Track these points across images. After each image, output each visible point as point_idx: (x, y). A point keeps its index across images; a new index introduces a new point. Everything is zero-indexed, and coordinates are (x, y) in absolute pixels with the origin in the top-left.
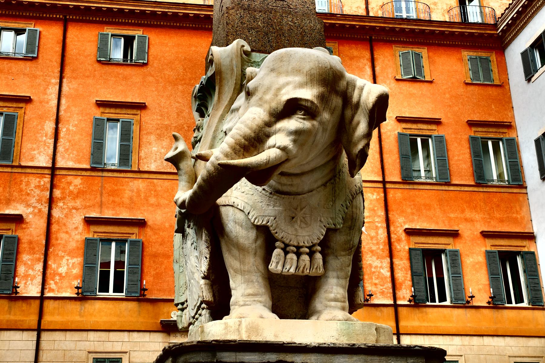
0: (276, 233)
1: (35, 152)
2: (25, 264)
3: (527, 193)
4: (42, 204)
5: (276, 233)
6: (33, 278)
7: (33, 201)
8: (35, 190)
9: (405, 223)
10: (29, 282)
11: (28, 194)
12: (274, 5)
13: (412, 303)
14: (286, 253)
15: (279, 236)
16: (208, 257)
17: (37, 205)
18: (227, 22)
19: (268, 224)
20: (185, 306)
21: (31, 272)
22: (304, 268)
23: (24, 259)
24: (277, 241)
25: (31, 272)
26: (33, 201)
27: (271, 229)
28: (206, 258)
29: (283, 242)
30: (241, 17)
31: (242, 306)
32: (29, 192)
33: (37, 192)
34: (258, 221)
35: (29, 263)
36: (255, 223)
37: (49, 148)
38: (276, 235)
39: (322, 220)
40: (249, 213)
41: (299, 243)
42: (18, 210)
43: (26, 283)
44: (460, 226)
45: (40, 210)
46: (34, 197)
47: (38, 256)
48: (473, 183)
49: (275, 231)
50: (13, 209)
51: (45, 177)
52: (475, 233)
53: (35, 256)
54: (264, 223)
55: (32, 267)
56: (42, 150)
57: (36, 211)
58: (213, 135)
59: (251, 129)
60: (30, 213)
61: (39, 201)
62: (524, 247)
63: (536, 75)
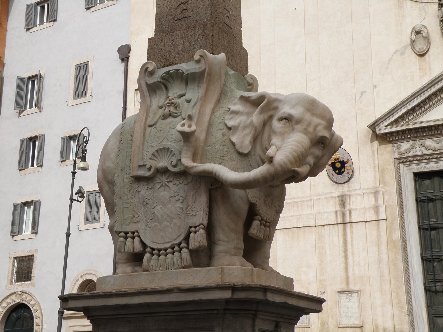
0: (259, 210)
5: (259, 210)
12: (228, 30)
14: (261, 224)
15: (261, 212)
16: (208, 214)
18: (213, 35)
19: (257, 203)
20: (128, 235)
22: (266, 236)
24: (257, 215)
27: (258, 207)
28: (207, 214)
29: (261, 217)
30: (218, 33)
31: (233, 255)
34: (252, 200)
36: (251, 201)
38: (259, 211)
39: (277, 206)
40: (248, 193)
41: (266, 219)
49: (259, 209)
54: (255, 202)
58: (209, 122)
59: (305, 149)
63: (35, 29)
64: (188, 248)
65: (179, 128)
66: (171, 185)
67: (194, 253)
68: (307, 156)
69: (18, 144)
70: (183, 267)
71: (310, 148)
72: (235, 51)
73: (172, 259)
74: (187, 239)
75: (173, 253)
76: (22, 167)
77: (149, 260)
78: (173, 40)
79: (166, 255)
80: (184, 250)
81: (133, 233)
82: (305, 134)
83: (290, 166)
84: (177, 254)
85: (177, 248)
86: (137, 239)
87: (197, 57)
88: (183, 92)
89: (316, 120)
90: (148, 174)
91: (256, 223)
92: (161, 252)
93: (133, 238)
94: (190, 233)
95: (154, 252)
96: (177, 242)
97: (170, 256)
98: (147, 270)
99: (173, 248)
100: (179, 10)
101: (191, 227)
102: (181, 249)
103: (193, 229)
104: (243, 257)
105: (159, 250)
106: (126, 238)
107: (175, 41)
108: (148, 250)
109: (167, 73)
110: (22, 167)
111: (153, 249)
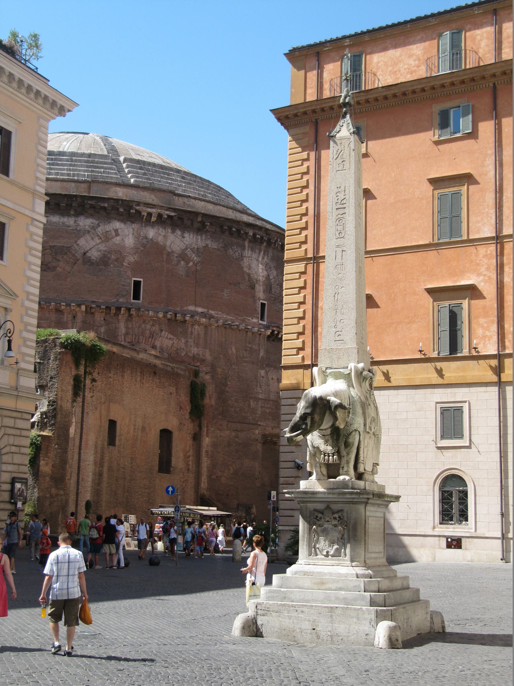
1: (480, 224)
2: (482, 327)
4: (491, 272)
6: (490, 338)
7: (483, 269)
8: (484, 260)
10: (487, 342)
11: (478, 264)
17: (486, 273)
21: (488, 333)
23: (481, 322)
25: (488, 333)
26: (483, 269)
32: (478, 262)
33: (485, 261)
35: (485, 325)
37: (491, 218)
42: (471, 279)
43: (484, 344)
45: (489, 277)
46: (483, 266)
47: (492, 318)
50: (467, 280)
51: (491, 246)
53: (489, 319)
55: (488, 329)
56: (486, 221)
57: (486, 278)
60: (481, 281)
61: (488, 269)
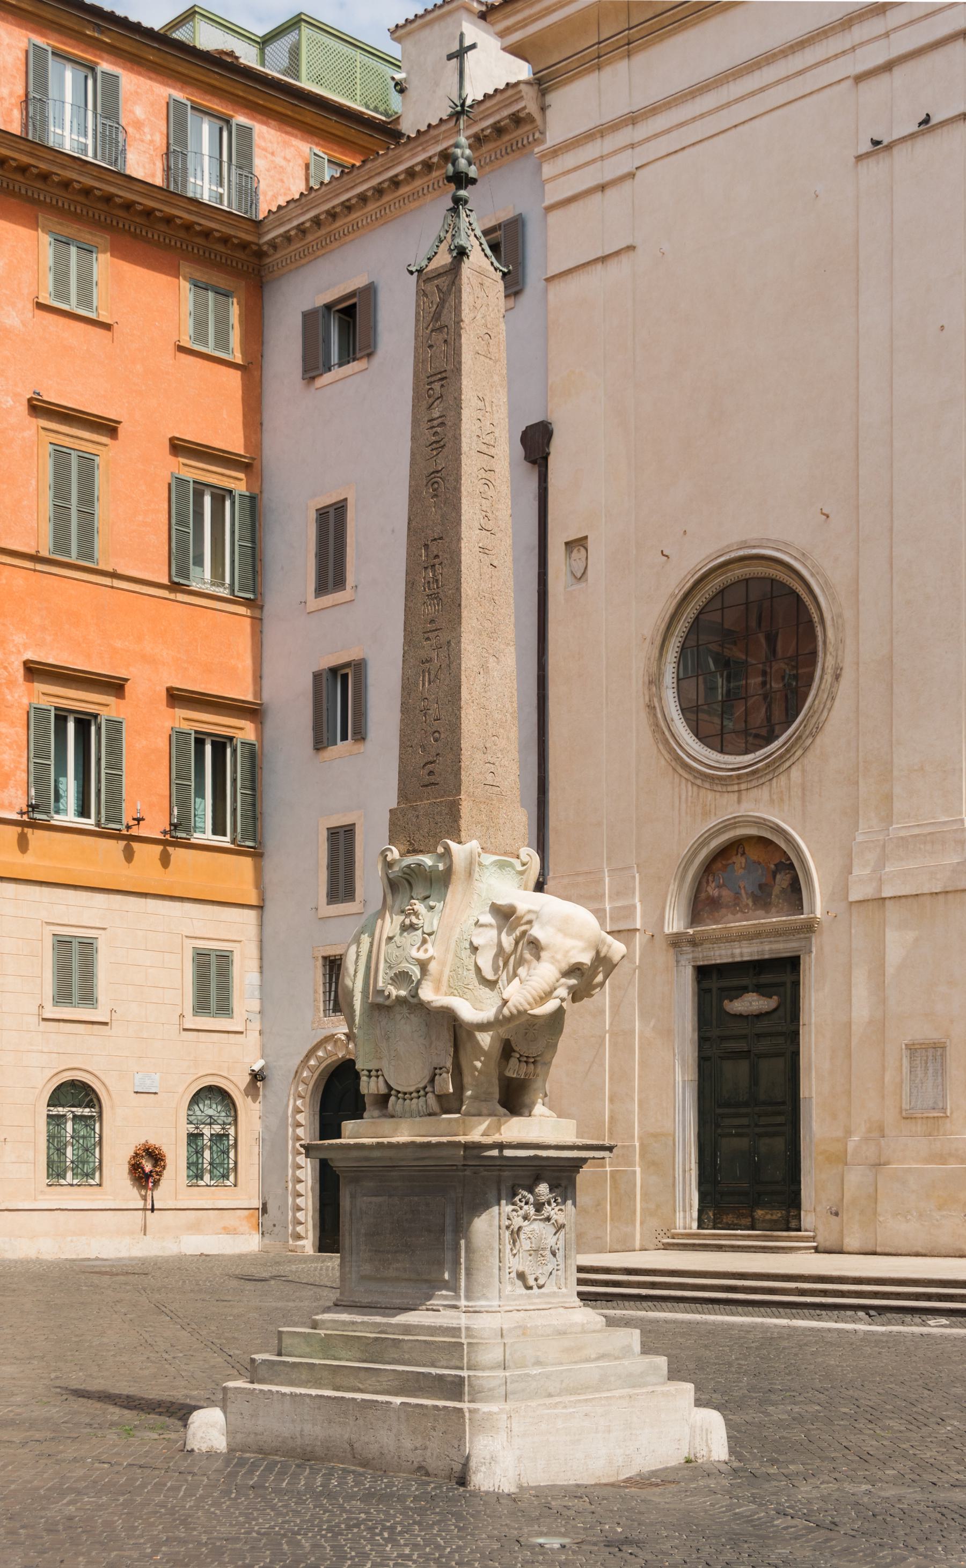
3: (261, 619)
9: (26, 646)
13: (25, 818)
14: (520, 1061)
24: (514, 1051)
44: (131, 669)
48: (165, 581)
52: (158, 688)
62: (241, 729)
64: (433, 1092)
65: (414, 953)
66: (412, 1016)
67: (440, 1098)
68: (555, 989)
69: (307, 683)
70: (430, 1115)
71: (557, 981)
72: (501, 821)
73: (417, 1104)
74: (432, 1081)
75: (419, 1097)
76: (320, 742)
77: (394, 1106)
78: (417, 816)
79: (411, 1099)
80: (430, 1095)
81: (377, 1071)
82: (552, 963)
83: (528, 1007)
84: (422, 1099)
85: (422, 1093)
86: (381, 1078)
87: (440, 850)
88: (427, 894)
89: (570, 942)
90: (387, 1003)
91: (513, 1062)
92: (407, 1096)
93: (377, 1077)
94: (435, 1075)
95: (400, 1095)
96: (422, 1085)
97: (415, 1101)
98: (393, 1117)
99: (418, 1092)
100: (426, 771)
101: (436, 1069)
102: (427, 1093)
103: (438, 1071)
104: (499, 1102)
105: (405, 1094)
106: (370, 1076)
107: (421, 817)
108: (393, 1092)
109: (408, 866)
110: (320, 742)
111: (399, 1092)
